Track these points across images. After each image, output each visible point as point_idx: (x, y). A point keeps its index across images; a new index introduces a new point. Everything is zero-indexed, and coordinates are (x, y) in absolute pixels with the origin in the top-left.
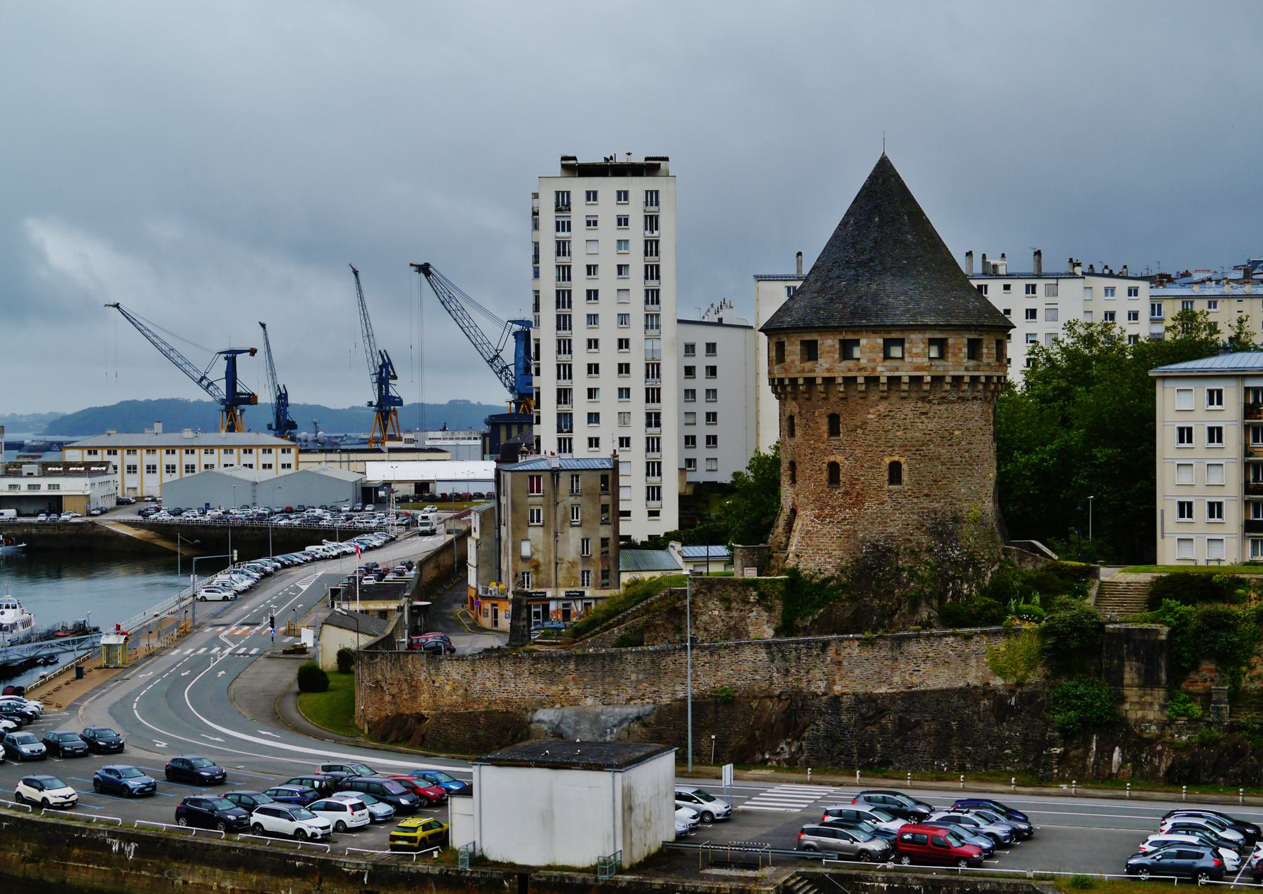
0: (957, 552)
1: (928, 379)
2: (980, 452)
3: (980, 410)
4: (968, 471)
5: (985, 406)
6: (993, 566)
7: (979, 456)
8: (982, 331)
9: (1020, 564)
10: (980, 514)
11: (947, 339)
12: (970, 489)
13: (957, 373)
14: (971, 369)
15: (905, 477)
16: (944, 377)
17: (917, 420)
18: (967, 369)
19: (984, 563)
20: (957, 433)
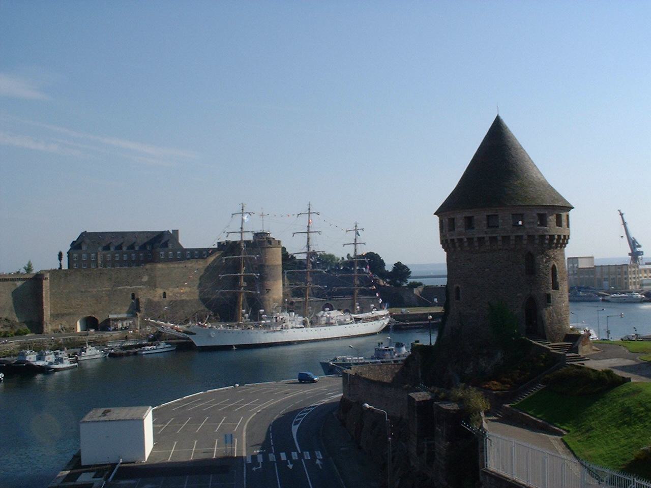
1: (465, 240)
11: (473, 217)
13: (480, 236)
15: (461, 296)
16: (473, 239)
17: (466, 263)
18: (486, 233)
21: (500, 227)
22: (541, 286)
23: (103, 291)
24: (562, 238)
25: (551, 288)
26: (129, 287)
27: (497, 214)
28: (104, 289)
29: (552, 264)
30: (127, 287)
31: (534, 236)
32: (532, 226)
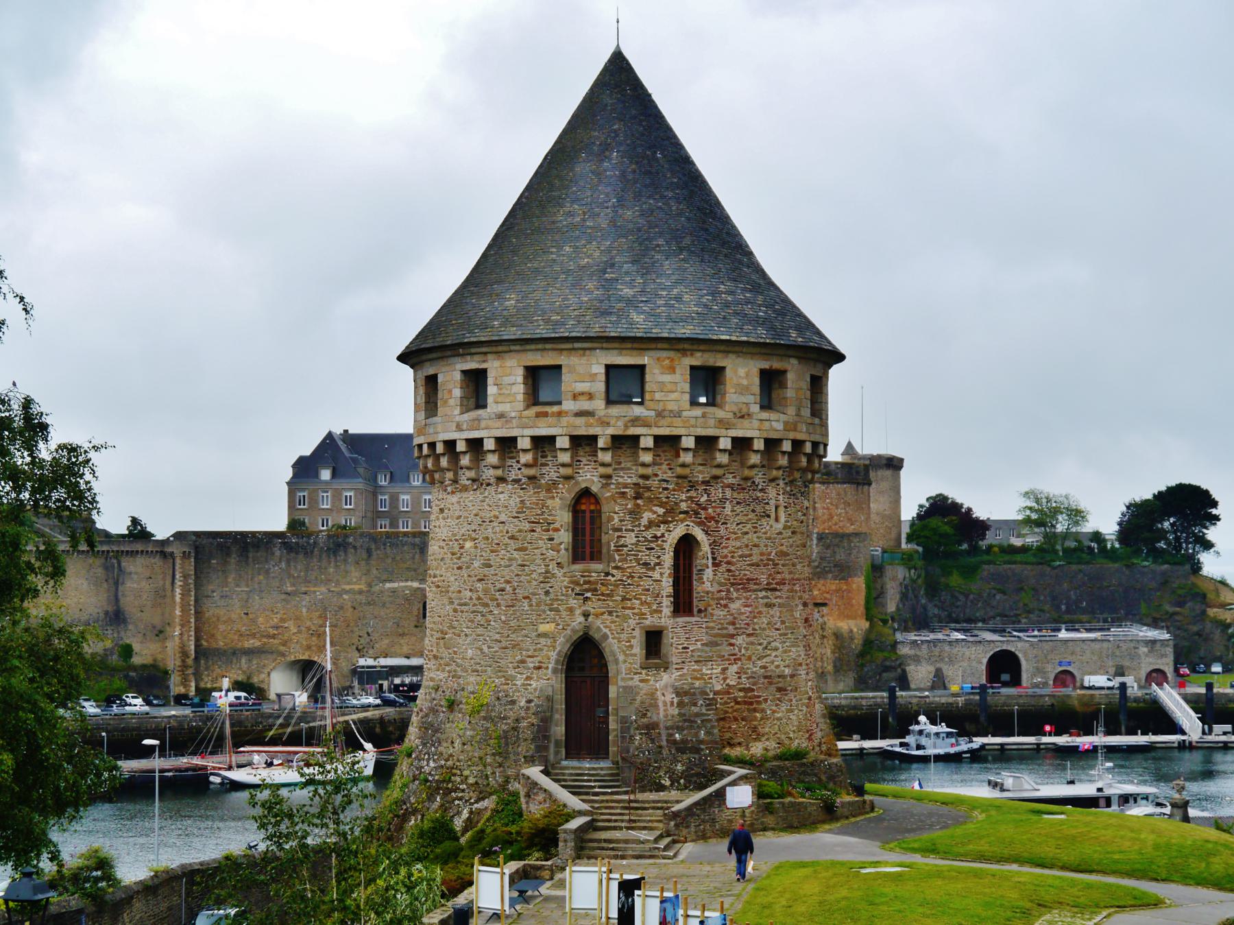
0: (432, 764)
2: (508, 582)
3: (514, 502)
4: (479, 618)
5: (530, 496)
6: (476, 802)
7: (503, 590)
8: (486, 353)
9: (527, 803)
10: (487, 697)
12: (481, 650)
14: (465, 427)
18: (459, 428)
19: (463, 791)
20: (468, 545)
21: (489, 410)
22: (629, 604)
23: (347, 592)
24: (787, 446)
25: (667, 610)
26: (415, 585)
27: (483, 366)
28: (347, 587)
29: (679, 531)
30: (409, 583)
31: (594, 438)
32: (585, 405)
